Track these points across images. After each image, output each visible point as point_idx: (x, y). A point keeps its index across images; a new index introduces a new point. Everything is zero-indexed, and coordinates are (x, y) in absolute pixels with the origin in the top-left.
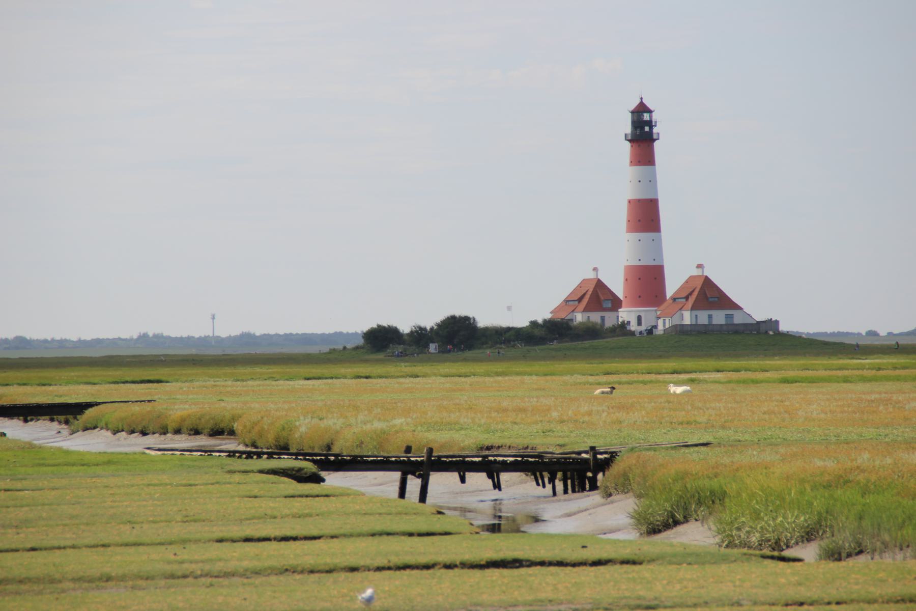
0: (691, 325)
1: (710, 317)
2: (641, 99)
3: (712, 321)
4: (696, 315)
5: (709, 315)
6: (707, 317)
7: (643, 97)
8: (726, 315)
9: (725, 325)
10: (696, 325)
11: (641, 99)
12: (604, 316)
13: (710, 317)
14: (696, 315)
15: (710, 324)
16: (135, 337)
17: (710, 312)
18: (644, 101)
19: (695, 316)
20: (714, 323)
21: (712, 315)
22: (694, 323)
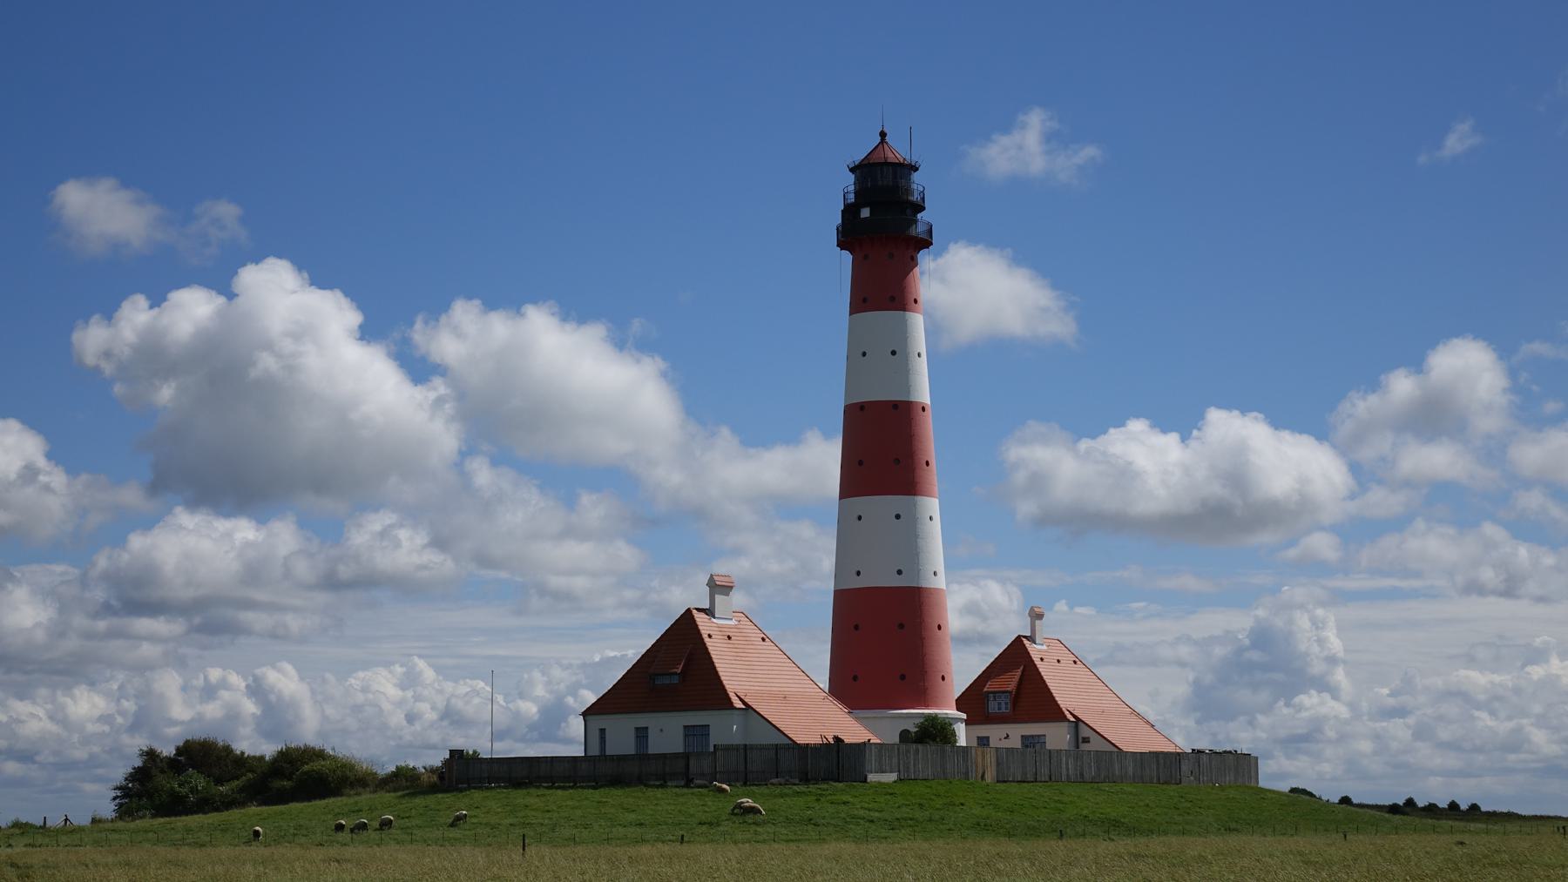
0: (586, 758)
1: (642, 734)
2: (883, 135)
4: (602, 731)
5: (637, 729)
7: (886, 130)
8: (685, 727)
10: (603, 757)
11: (883, 135)
13: (642, 734)
14: (602, 731)
15: (642, 757)
17: (641, 720)
19: (597, 733)
20: (650, 752)
22: (594, 751)
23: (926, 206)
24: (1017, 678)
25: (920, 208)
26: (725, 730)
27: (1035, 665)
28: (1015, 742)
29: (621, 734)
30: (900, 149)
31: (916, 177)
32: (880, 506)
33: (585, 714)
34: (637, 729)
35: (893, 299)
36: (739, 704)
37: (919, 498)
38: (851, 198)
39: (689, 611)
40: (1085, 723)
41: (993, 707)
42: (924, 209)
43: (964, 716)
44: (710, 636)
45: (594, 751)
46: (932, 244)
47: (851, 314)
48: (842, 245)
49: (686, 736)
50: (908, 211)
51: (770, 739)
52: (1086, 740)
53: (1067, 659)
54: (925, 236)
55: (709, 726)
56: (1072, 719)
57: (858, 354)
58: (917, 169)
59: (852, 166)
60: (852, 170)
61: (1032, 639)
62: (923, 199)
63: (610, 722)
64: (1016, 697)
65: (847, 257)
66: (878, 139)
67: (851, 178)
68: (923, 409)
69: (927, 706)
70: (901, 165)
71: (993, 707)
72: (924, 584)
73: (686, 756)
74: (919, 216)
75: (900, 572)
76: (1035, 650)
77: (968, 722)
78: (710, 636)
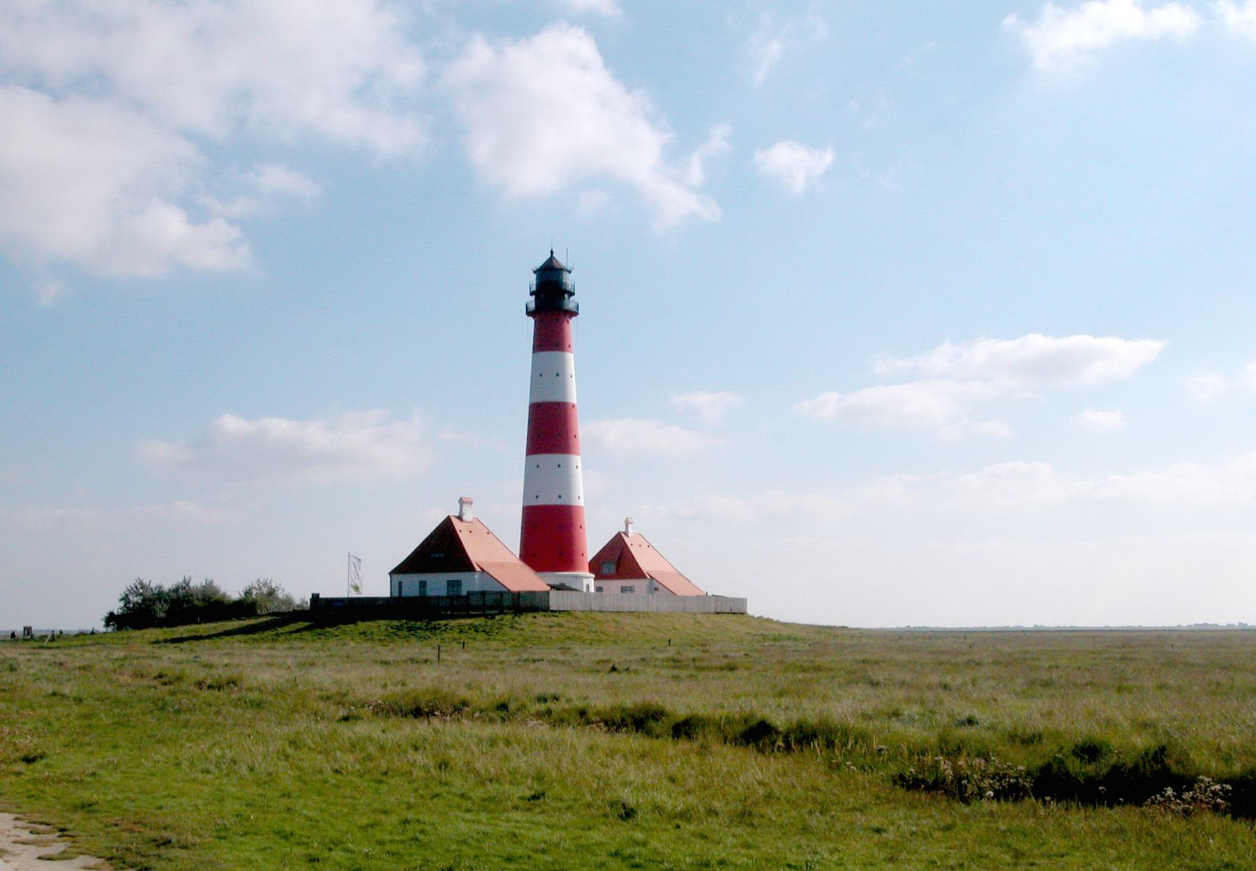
0: (392, 599)
1: (423, 585)
2: (552, 252)
3: (425, 592)
5: (421, 582)
6: (417, 583)
7: (554, 251)
8: (448, 581)
9: (446, 597)
10: (400, 597)
11: (552, 252)
12: (425, 582)
13: (423, 585)
14: (400, 583)
16: (756, 616)
18: (554, 255)
19: (398, 584)
21: (448, 581)
22: (396, 594)
23: (576, 292)
25: (571, 294)
26: (470, 583)
27: (628, 548)
29: (411, 585)
30: (561, 259)
32: (547, 460)
33: (390, 573)
34: (421, 582)
36: (478, 569)
38: (534, 288)
39: (449, 518)
40: (657, 581)
41: (605, 571)
42: (573, 294)
44: (460, 531)
46: (578, 314)
47: (533, 353)
48: (529, 313)
49: (448, 586)
50: (566, 296)
51: (497, 588)
53: (644, 545)
54: (575, 310)
56: (649, 577)
57: (538, 376)
59: (535, 270)
60: (535, 272)
61: (626, 533)
65: (531, 321)
66: (550, 255)
67: (534, 276)
70: (562, 270)
71: (605, 571)
73: (449, 597)
74: (571, 298)
75: (560, 497)
77: (595, 579)
78: (460, 531)
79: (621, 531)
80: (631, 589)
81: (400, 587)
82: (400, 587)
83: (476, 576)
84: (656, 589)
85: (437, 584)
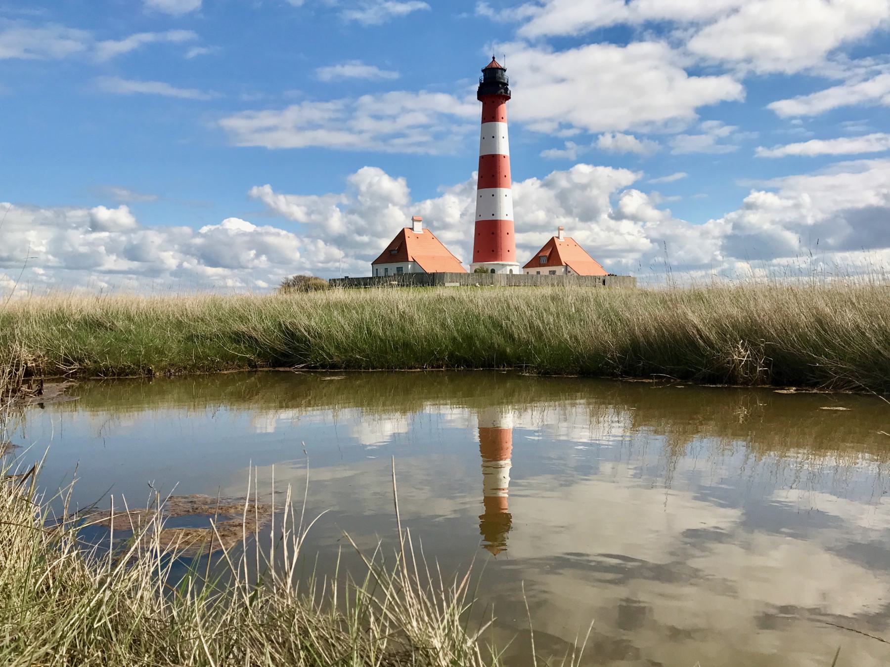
1: (386, 270)
13: (386, 270)
22: (375, 276)
24: (549, 252)
28: (547, 273)
30: (501, 63)
31: (506, 74)
33: (372, 264)
35: (493, 118)
37: (498, 189)
39: (404, 229)
43: (519, 264)
45: (375, 276)
47: (482, 123)
50: (500, 86)
52: (569, 272)
55: (402, 267)
56: (564, 264)
58: (505, 71)
60: (483, 71)
61: (558, 238)
62: (508, 82)
63: (379, 266)
64: (549, 258)
66: (492, 60)
68: (504, 157)
69: (502, 261)
71: (542, 262)
72: (502, 219)
76: (557, 242)
79: (554, 236)
80: (554, 272)
81: (377, 272)
82: (377, 272)
83: (410, 266)
84: (569, 272)
85: (392, 268)
